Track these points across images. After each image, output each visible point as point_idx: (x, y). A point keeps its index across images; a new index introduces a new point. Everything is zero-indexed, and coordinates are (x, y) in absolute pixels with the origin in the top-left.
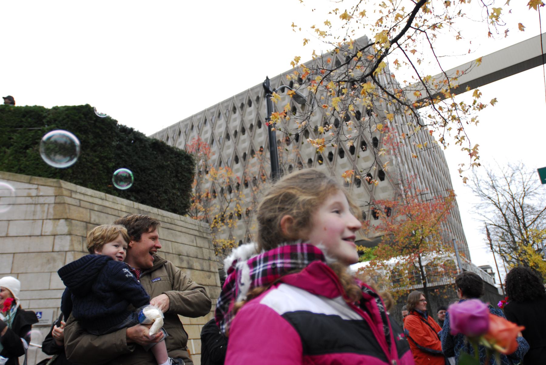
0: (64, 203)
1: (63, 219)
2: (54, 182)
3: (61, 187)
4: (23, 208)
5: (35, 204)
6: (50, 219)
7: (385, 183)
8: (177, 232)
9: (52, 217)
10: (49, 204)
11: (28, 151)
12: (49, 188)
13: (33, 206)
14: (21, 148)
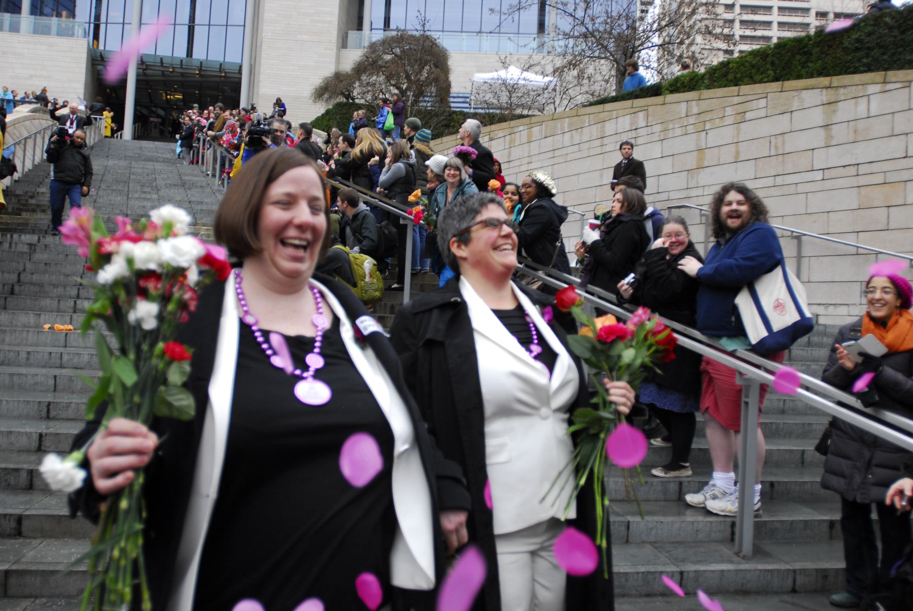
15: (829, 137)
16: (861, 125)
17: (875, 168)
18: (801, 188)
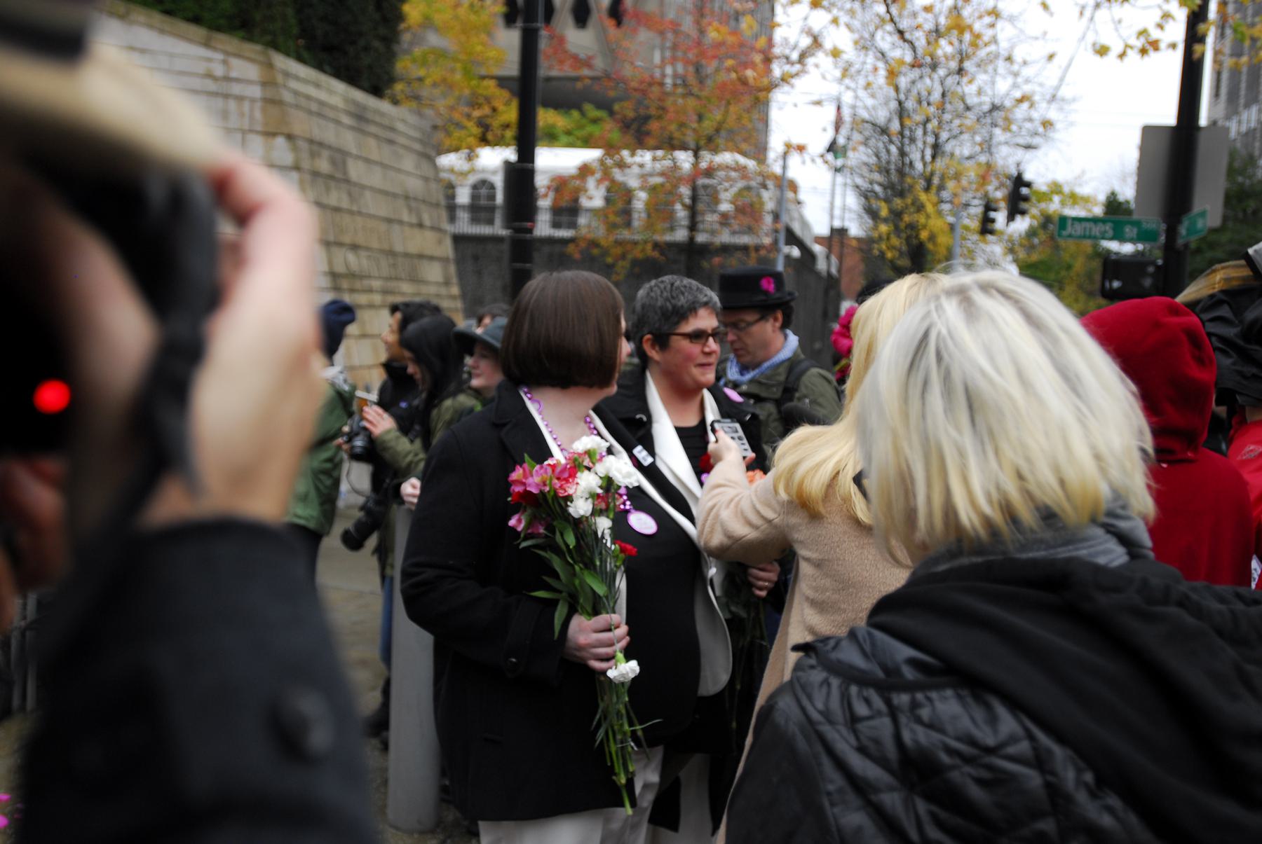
1: (282, 134)
3: (270, 66)
6: (257, 132)
8: (401, 151)
9: (259, 128)
10: (253, 100)
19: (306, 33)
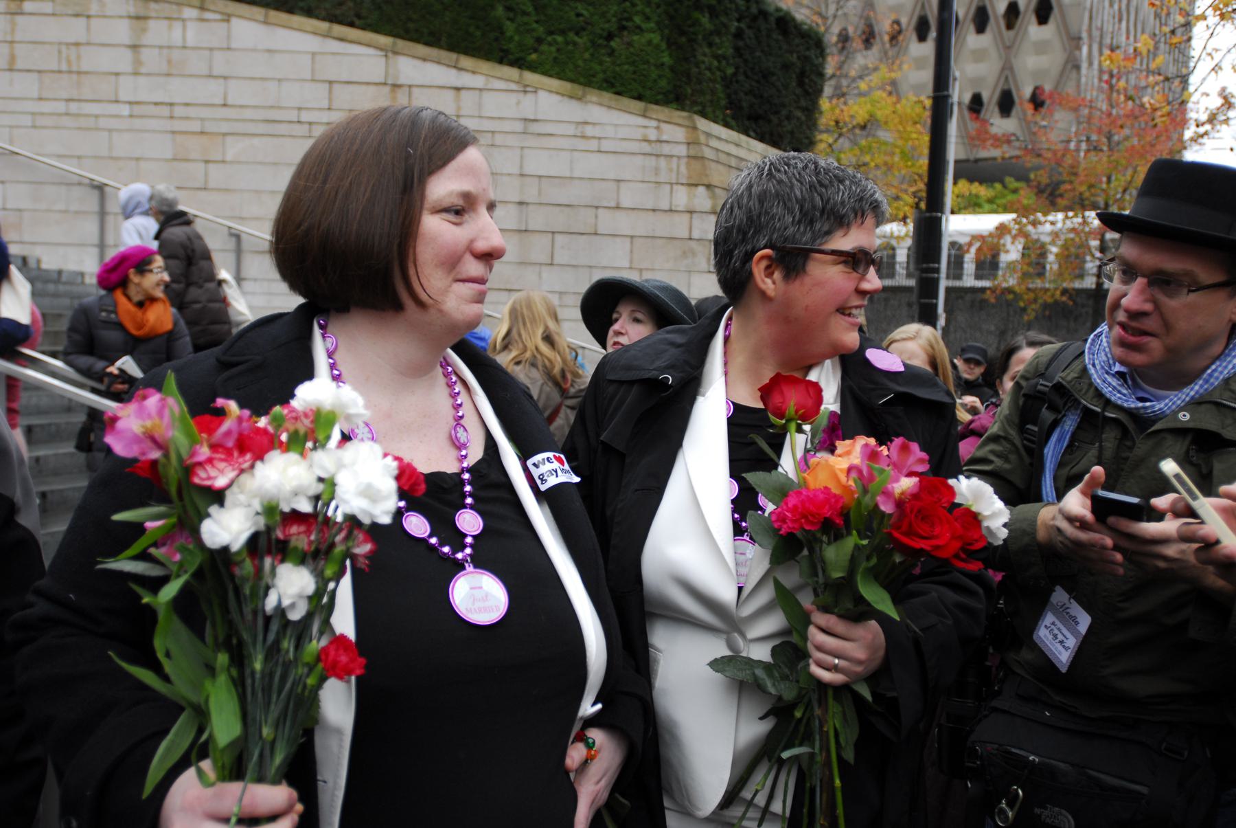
0: (703, 158)
2: (684, 118)
3: (695, 128)
4: (639, 160)
5: (658, 156)
7: (1047, 32)
9: (684, 181)
10: (679, 157)
11: (613, 44)
12: (677, 129)
13: (653, 158)
14: (601, 37)
15: (138, 62)
16: (176, 55)
17: (192, 112)
18: (103, 123)
19: (733, 105)
